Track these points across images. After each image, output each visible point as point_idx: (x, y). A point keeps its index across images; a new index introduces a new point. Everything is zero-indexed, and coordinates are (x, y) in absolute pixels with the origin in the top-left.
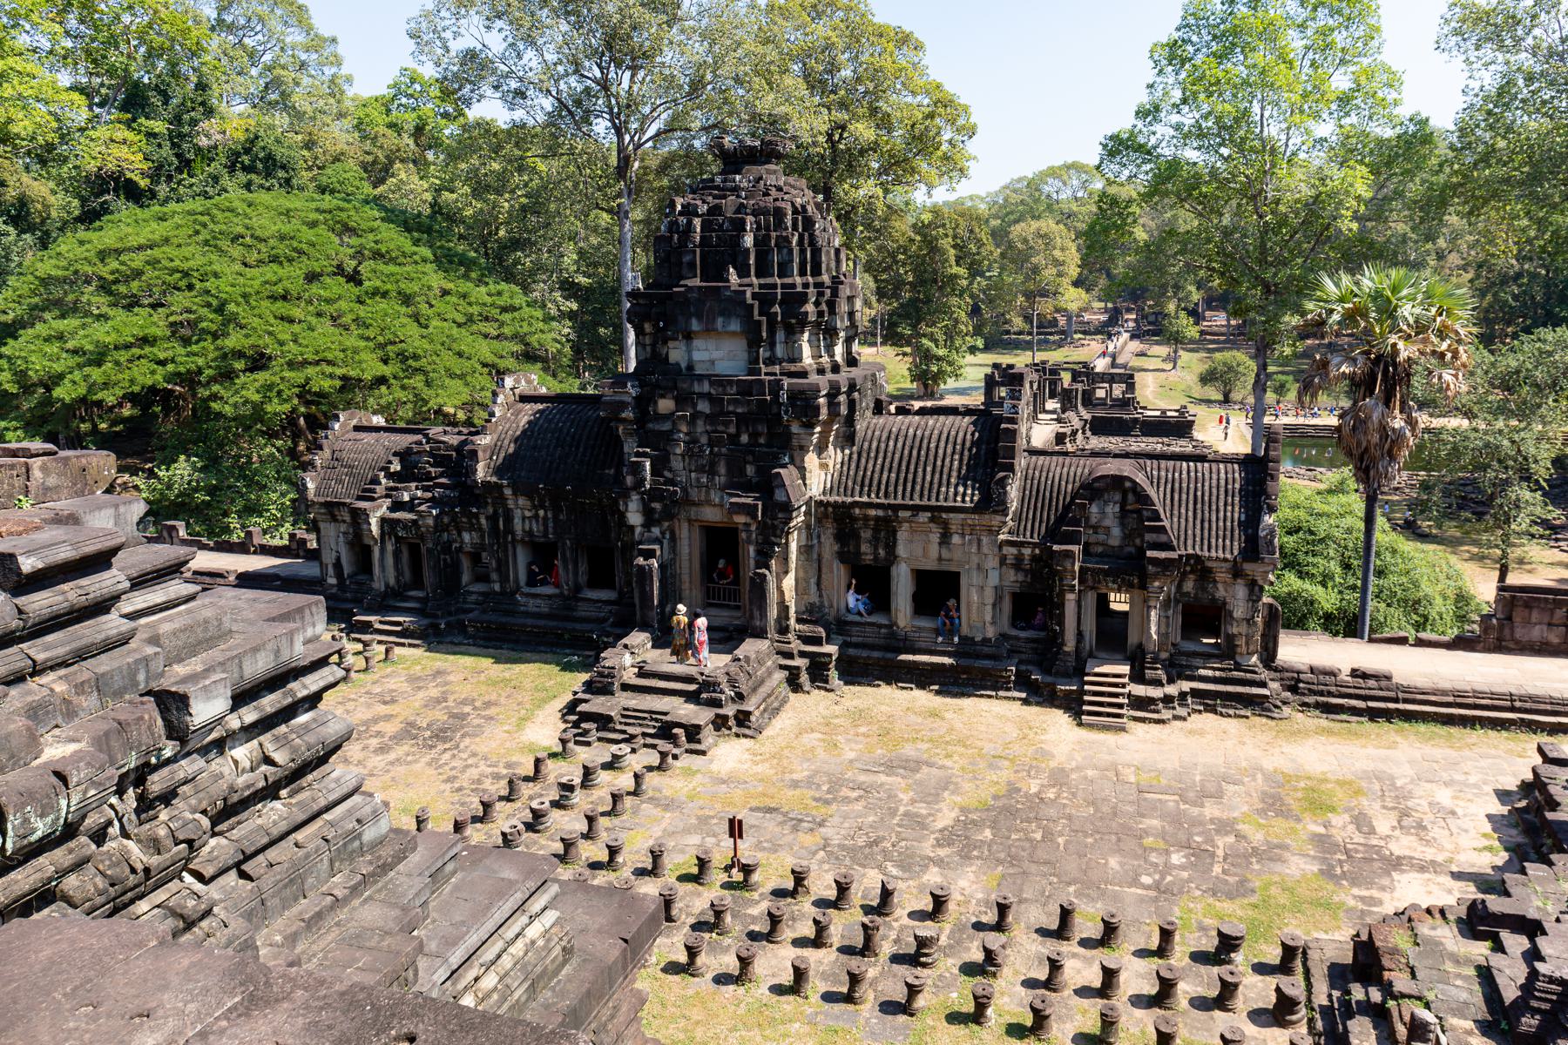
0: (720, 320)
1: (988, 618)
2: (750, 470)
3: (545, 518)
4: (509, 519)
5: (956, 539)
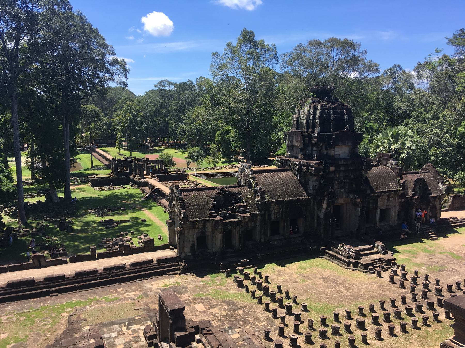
0: (347, 142)
1: (396, 219)
2: (354, 186)
3: (282, 212)
4: (270, 214)
5: (390, 199)
